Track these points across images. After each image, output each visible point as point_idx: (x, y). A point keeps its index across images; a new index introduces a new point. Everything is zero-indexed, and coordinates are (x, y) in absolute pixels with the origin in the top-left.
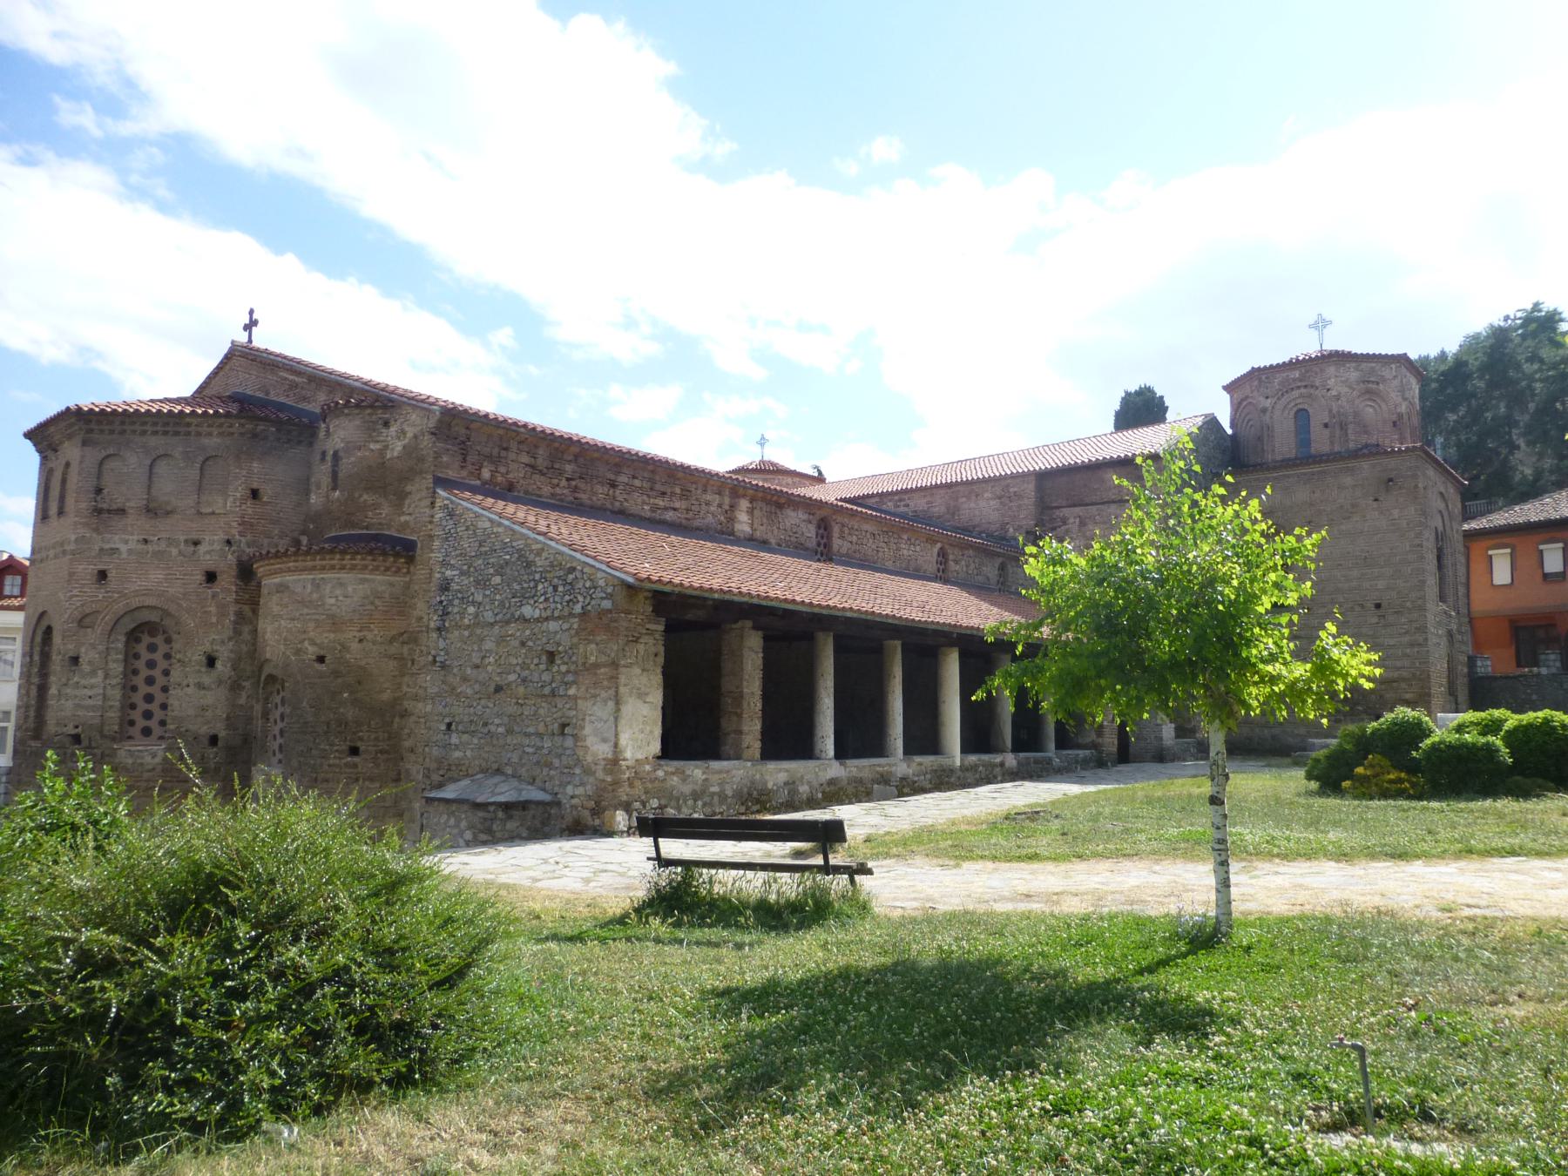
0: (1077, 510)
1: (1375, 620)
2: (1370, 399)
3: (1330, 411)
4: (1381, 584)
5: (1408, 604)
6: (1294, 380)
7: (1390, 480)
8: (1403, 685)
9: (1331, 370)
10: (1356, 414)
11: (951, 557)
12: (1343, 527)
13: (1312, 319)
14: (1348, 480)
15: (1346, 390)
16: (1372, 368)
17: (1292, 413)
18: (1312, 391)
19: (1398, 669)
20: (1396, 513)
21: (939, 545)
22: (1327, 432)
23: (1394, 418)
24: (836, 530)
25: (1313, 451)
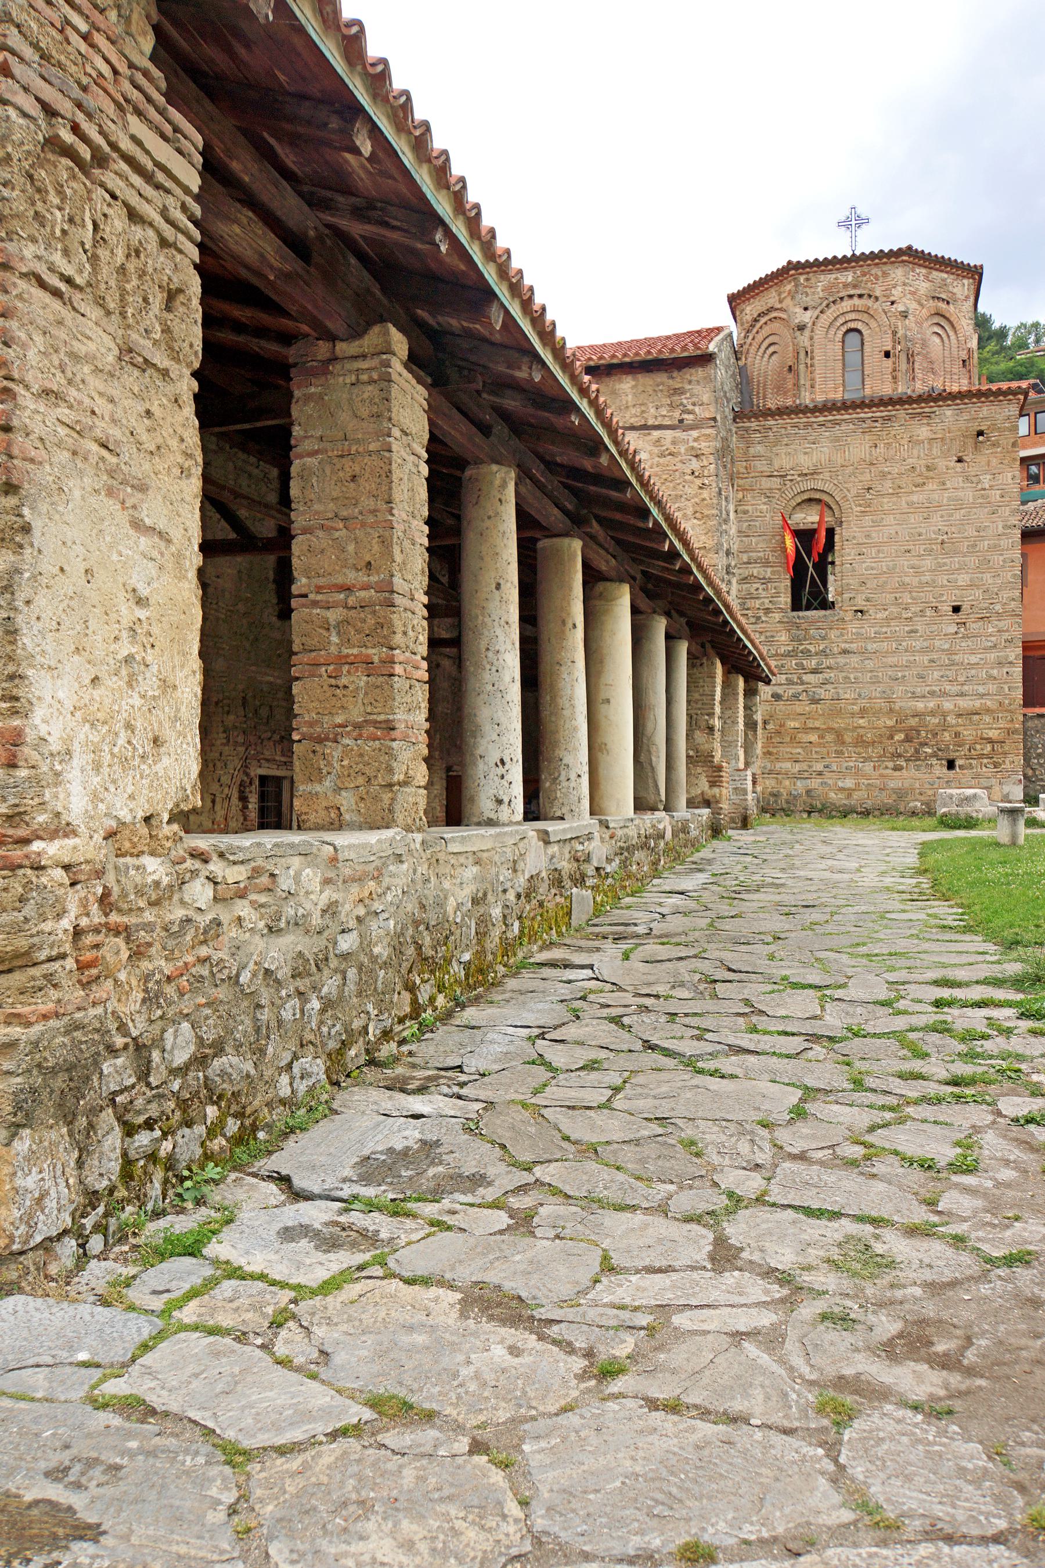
1: (953, 629)
3: (895, 333)
4: (963, 579)
5: (998, 607)
6: (846, 285)
7: (980, 433)
8: (987, 719)
9: (898, 273)
10: (924, 344)
12: (915, 498)
13: (843, 214)
14: (923, 432)
16: (944, 280)
18: (870, 303)
19: (982, 696)
20: (986, 480)
22: (888, 363)
25: (868, 392)
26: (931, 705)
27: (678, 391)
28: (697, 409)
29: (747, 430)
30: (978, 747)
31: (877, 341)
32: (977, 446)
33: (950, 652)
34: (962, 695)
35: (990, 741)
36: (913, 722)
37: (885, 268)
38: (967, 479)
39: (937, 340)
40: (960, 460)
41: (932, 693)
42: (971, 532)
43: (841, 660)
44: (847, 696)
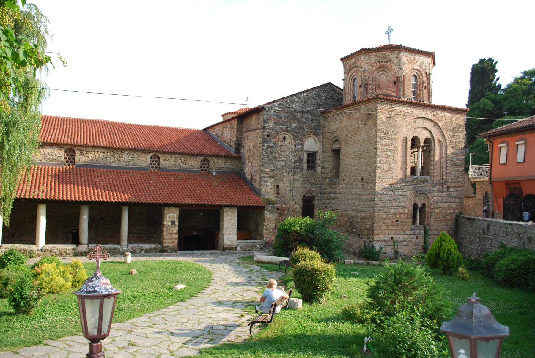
0: (247, 133)
1: (360, 187)
2: (382, 71)
3: (362, 78)
4: (364, 168)
7: (370, 114)
8: (367, 220)
9: (363, 57)
11: (161, 158)
12: (355, 139)
14: (357, 115)
15: (369, 67)
17: (353, 80)
19: (366, 212)
21: (152, 154)
23: (395, 80)
24: (78, 153)
26: (355, 214)
27: (259, 119)
28: (261, 124)
29: (325, 117)
30: (364, 231)
31: (358, 82)
32: (368, 118)
33: (360, 195)
34: (362, 211)
35: (367, 229)
36: (351, 219)
37: (361, 56)
38: (366, 132)
39: (384, 76)
40: (365, 125)
41: (355, 209)
42: (366, 151)
43: (338, 196)
44: (339, 209)
